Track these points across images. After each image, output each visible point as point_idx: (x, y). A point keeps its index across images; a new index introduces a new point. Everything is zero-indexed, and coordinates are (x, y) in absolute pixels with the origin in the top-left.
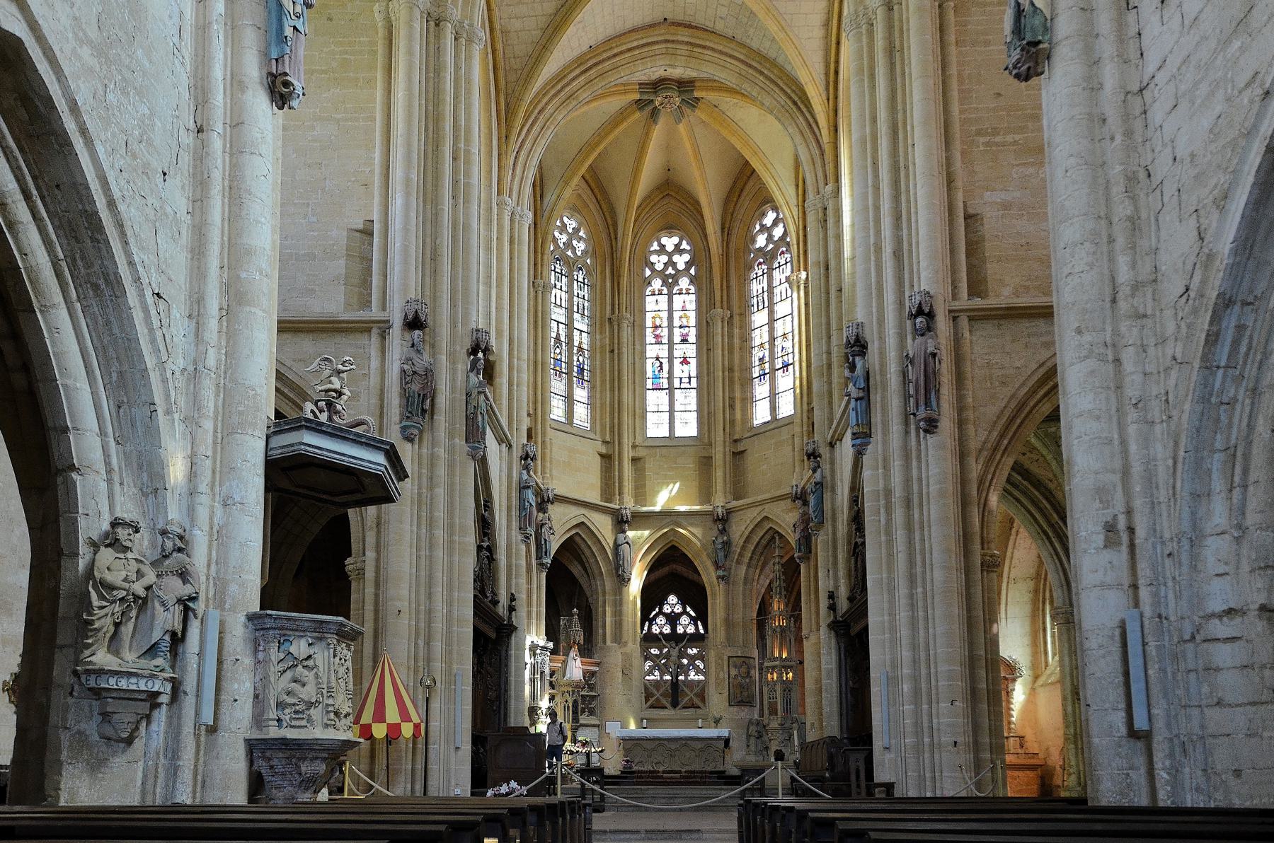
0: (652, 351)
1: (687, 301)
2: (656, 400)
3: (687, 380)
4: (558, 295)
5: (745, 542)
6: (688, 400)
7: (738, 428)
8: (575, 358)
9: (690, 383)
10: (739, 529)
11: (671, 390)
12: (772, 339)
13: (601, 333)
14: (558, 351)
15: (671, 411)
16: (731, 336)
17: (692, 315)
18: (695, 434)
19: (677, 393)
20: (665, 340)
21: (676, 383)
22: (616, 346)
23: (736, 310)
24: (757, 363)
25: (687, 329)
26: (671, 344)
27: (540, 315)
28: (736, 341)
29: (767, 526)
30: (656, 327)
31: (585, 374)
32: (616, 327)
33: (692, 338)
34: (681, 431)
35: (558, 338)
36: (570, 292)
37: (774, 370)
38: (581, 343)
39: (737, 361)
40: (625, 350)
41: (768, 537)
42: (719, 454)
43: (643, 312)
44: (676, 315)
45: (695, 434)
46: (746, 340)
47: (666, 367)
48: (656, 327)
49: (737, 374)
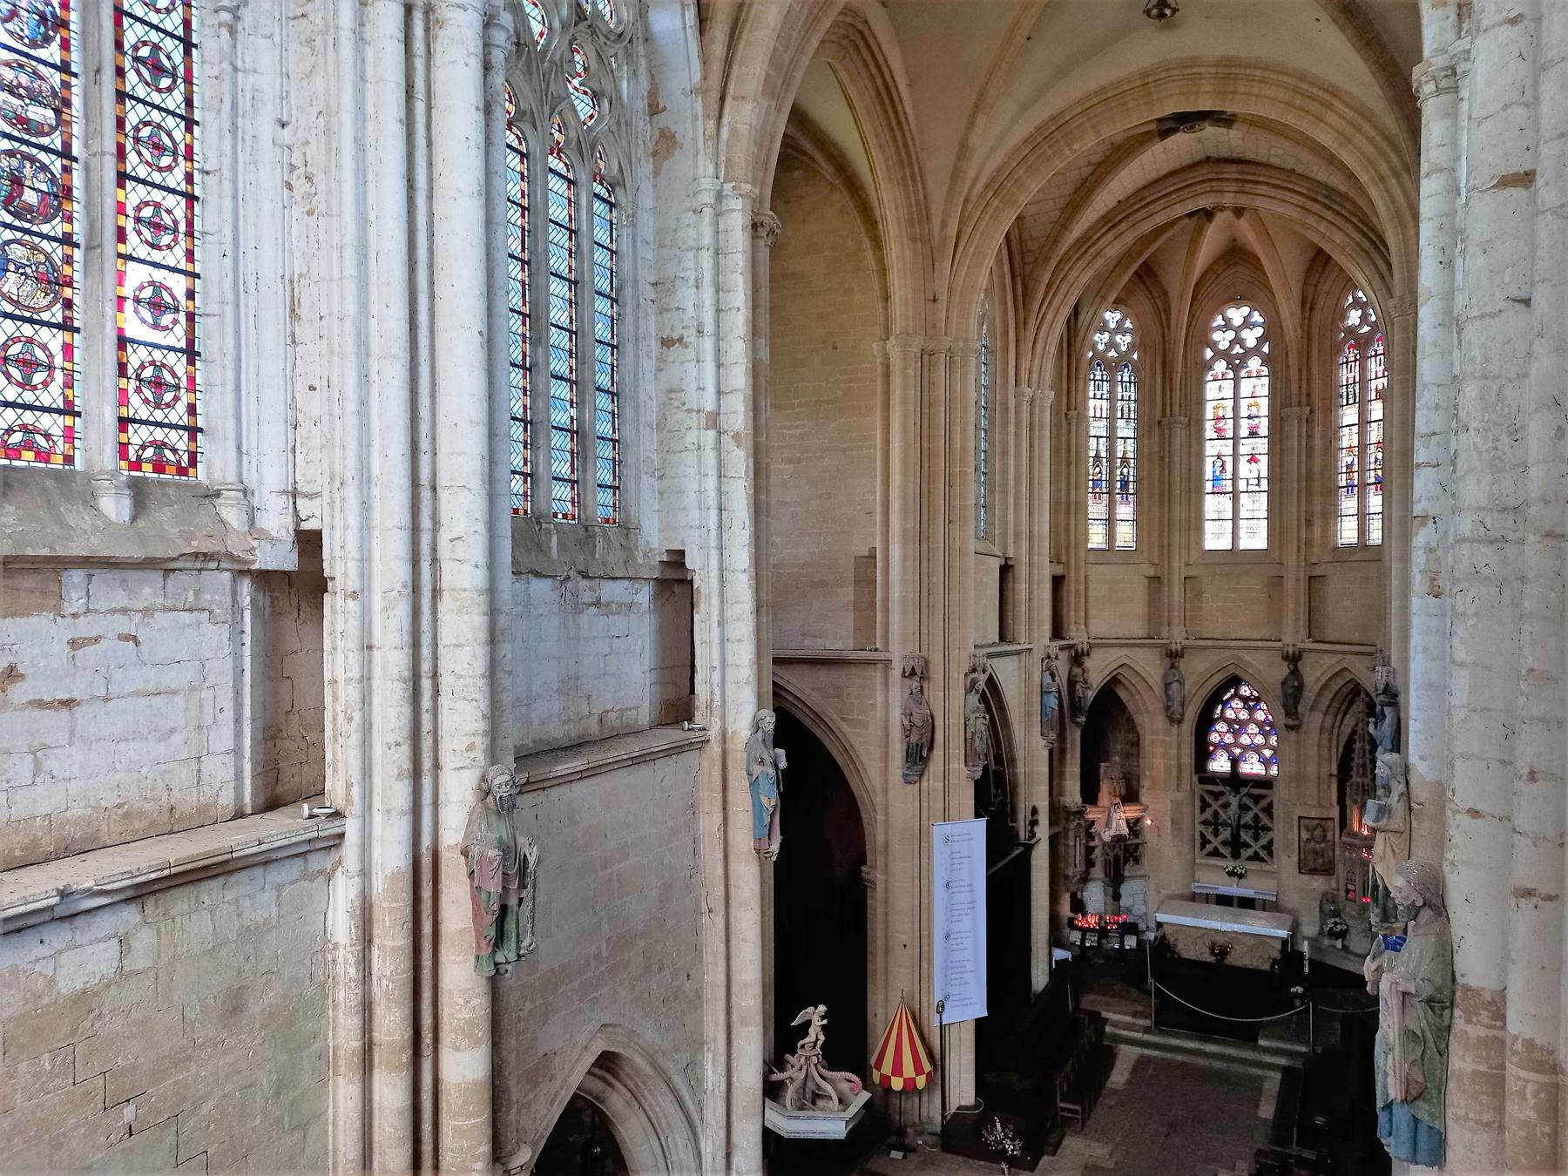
0: (1212, 448)
1: (1257, 385)
2: (1215, 506)
3: (1256, 482)
4: (1096, 406)
5: (1321, 689)
6: (1256, 506)
7: (1316, 549)
8: (1118, 472)
9: (1258, 485)
10: (1315, 673)
12: (1363, 446)
13: (1150, 438)
14: (1098, 470)
16: (1310, 436)
17: (1264, 403)
18: (1265, 547)
19: (1244, 498)
21: (1242, 486)
22: (1167, 454)
23: (1317, 403)
24: (1344, 470)
25: (1257, 420)
26: (1236, 439)
27: (1073, 449)
28: (1318, 443)
29: (1348, 677)
31: (1131, 486)
32: (1167, 432)
33: (1263, 431)
34: (1245, 543)
35: (1097, 457)
36: (1112, 399)
37: (1363, 486)
38: (1125, 452)
39: (1317, 468)
40: (1177, 459)
41: (1351, 686)
42: (1294, 586)
43: (1201, 402)
44: (1244, 404)
45: (1265, 547)
47: (1229, 467)
48: (1217, 419)
49: (1317, 483)
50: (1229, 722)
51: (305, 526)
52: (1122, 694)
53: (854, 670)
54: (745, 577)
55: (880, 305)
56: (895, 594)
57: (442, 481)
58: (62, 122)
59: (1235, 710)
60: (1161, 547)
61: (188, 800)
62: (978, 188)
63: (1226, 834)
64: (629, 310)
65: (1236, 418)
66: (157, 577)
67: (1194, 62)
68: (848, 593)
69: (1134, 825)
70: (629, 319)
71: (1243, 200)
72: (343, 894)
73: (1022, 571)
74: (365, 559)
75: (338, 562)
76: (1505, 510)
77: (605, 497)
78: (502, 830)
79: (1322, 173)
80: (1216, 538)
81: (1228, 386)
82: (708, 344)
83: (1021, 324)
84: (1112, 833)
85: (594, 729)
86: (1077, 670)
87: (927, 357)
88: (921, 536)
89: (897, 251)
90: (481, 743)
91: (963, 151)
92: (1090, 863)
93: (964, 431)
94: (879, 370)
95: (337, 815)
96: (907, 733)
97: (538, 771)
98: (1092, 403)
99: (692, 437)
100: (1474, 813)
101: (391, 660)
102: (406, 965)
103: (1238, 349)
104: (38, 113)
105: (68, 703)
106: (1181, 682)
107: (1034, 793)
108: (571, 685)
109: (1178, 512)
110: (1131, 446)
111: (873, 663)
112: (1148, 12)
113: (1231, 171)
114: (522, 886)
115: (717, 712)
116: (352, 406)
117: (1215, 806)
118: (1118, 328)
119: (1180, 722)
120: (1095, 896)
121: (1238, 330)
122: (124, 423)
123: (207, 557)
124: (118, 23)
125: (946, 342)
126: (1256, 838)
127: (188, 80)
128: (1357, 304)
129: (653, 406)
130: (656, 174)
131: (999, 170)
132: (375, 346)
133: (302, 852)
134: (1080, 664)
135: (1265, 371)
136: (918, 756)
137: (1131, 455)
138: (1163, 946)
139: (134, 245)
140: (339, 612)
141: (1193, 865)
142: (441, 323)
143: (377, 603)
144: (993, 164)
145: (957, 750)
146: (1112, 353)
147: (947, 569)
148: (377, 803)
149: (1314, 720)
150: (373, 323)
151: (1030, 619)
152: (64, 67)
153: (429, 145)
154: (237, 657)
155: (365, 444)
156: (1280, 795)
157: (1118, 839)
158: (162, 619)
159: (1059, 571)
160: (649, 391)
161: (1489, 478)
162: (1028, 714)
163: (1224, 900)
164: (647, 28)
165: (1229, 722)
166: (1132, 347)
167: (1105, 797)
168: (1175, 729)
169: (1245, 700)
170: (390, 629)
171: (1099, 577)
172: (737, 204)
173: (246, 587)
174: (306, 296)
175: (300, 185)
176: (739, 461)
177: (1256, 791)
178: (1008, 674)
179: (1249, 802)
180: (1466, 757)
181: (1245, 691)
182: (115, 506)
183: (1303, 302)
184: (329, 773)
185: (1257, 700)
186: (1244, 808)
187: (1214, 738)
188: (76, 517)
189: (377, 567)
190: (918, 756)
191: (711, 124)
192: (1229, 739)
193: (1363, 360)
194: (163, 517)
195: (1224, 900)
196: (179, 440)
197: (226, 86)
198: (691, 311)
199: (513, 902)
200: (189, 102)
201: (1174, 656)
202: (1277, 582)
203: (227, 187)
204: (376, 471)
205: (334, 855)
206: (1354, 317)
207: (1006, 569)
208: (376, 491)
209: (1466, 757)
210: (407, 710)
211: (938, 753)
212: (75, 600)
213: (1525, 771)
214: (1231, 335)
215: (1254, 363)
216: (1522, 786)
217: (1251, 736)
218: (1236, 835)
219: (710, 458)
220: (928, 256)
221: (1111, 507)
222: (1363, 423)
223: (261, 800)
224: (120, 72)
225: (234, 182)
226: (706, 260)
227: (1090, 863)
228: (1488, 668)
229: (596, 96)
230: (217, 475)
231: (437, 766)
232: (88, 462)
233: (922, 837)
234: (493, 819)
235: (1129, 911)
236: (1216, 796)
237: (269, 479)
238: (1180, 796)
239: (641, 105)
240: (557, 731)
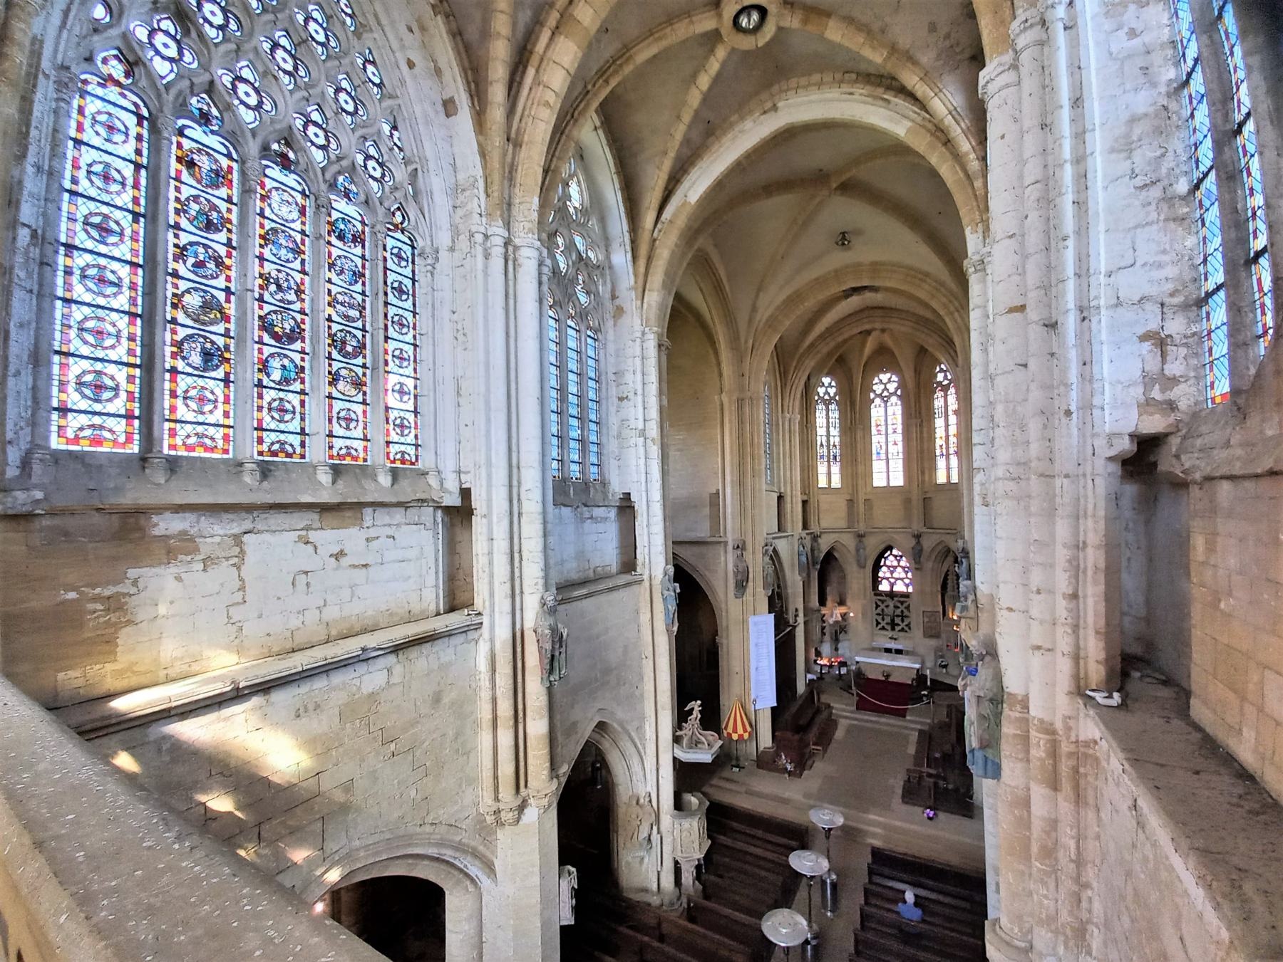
0: (875, 439)
1: (896, 409)
2: (878, 466)
4: (820, 419)
6: (897, 467)
10: (928, 543)
11: (887, 460)
12: (947, 437)
15: (888, 472)
16: (921, 432)
20: (883, 432)
21: (890, 456)
26: (887, 434)
28: (925, 435)
30: (877, 426)
33: (900, 429)
35: (822, 445)
37: (948, 455)
46: (932, 438)
47: (884, 447)
50: (888, 567)
51: (464, 486)
52: (836, 554)
53: (710, 547)
54: (659, 504)
55: (717, 379)
56: (729, 510)
57: (522, 464)
58: (362, 316)
59: (891, 561)
60: (853, 486)
61: (416, 608)
62: (761, 324)
63: (888, 619)
64: (604, 385)
65: (886, 425)
66: (402, 510)
67: (859, 264)
68: (707, 511)
69: (844, 616)
70: (604, 390)
71: (885, 326)
72: (483, 649)
73: (788, 499)
74: (489, 500)
75: (477, 502)
76: (1019, 464)
77: (594, 469)
78: (551, 621)
79: (922, 311)
80: (879, 481)
81: (882, 410)
82: (640, 398)
83: (783, 386)
84: (834, 619)
85: (591, 574)
86: (815, 544)
87: (740, 402)
88: (741, 483)
89: (725, 354)
90: (541, 582)
91: (754, 309)
92: (823, 634)
93: (759, 435)
94: (718, 407)
95: (480, 614)
96: (736, 574)
97: (567, 595)
98: (818, 420)
99: (632, 441)
100: (1010, 609)
101: (501, 545)
102: (511, 681)
103: (885, 393)
104: (354, 313)
105: (365, 566)
106: (864, 549)
107: (796, 602)
108: (581, 555)
109: (861, 469)
110: (837, 440)
111: (720, 543)
112: (837, 243)
113: (879, 312)
114: (561, 646)
115: (647, 566)
116: (483, 432)
117: (882, 606)
118: (830, 385)
119: (864, 567)
120: (826, 648)
121: (885, 384)
122: (388, 443)
123: (423, 501)
124: (385, 273)
125: (749, 394)
126: (903, 621)
127: (414, 296)
128: (942, 370)
129: (615, 427)
130: (615, 325)
131: (771, 316)
132: (492, 404)
133: (464, 630)
134: (816, 541)
135: (899, 403)
136: (741, 585)
137: (837, 444)
138: (859, 674)
139: (392, 366)
140: (478, 523)
141: (873, 635)
142: (521, 395)
143: (495, 519)
144: (767, 315)
145: (760, 583)
146: (827, 397)
147: (754, 497)
148: (496, 609)
149: (929, 565)
150: (492, 395)
151: (793, 521)
152: (363, 293)
153: (515, 318)
154: (436, 545)
155: (489, 449)
156: (913, 602)
157: (836, 622)
158: (405, 528)
159: (805, 498)
160: (613, 421)
161: (1010, 449)
162: (793, 565)
163: (888, 651)
164: (610, 262)
165: (888, 567)
166: (836, 394)
167: (829, 603)
168: (862, 570)
169: (895, 556)
170: (501, 531)
171: (824, 499)
172: (652, 336)
173: (439, 513)
174: (464, 384)
175: (461, 338)
176: (655, 451)
177: (902, 599)
178: (782, 546)
179: (899, 605)
180: (1005, 582)
181: (895, 552)
182: (385, 480)
183: (915, 371)
184: (475, 595)
185: (901, 557)
186: (896, 607)
187: (881, 574)
188: (369, 485)
189: (494, 503)
190: (741, 585)
191: (639, 303)
192: (888, 575)
193: (946, 397)
194: (404, 483)
195: (888, 651)
196: (411, 450)
197: (430, 297)
198: (631, 383)
199: (557, 654)
200: (414, 305)
201: (860, 536)
202: (907, 502)
203: (431, 340)
204: (494, 460)
205: (479, 632)
206: (940, 377)
207: (780, 498)
208: (494, 470)
209: (1005, 582)
210: (508, 567)
211: (750, 584)
212: (368, 521)
213: (1035, 589)
214: (882, 387)
215: (894, 399)
216: (1036, 597)
217: (899, 573)
218: (893, 620)
219: (642, 450)
220: (739, 357)
221: (829, 466)
222: (947, 426)
223: (447, 607)
224: (386, 294)
225: (434, 338)
226: (638, 361)
227: (823, 634)
228: (1014, 539)
229: (588, 293)
230: (427, 465)
231: (522, 592)
232: (373, 461)
233: (744, 622)
234: (547, 616)
235: (843, 656)
236: (883, 602)
237: (448, 466)
238: (865, 602)
239: (608, 296)
240: (574, 576)
